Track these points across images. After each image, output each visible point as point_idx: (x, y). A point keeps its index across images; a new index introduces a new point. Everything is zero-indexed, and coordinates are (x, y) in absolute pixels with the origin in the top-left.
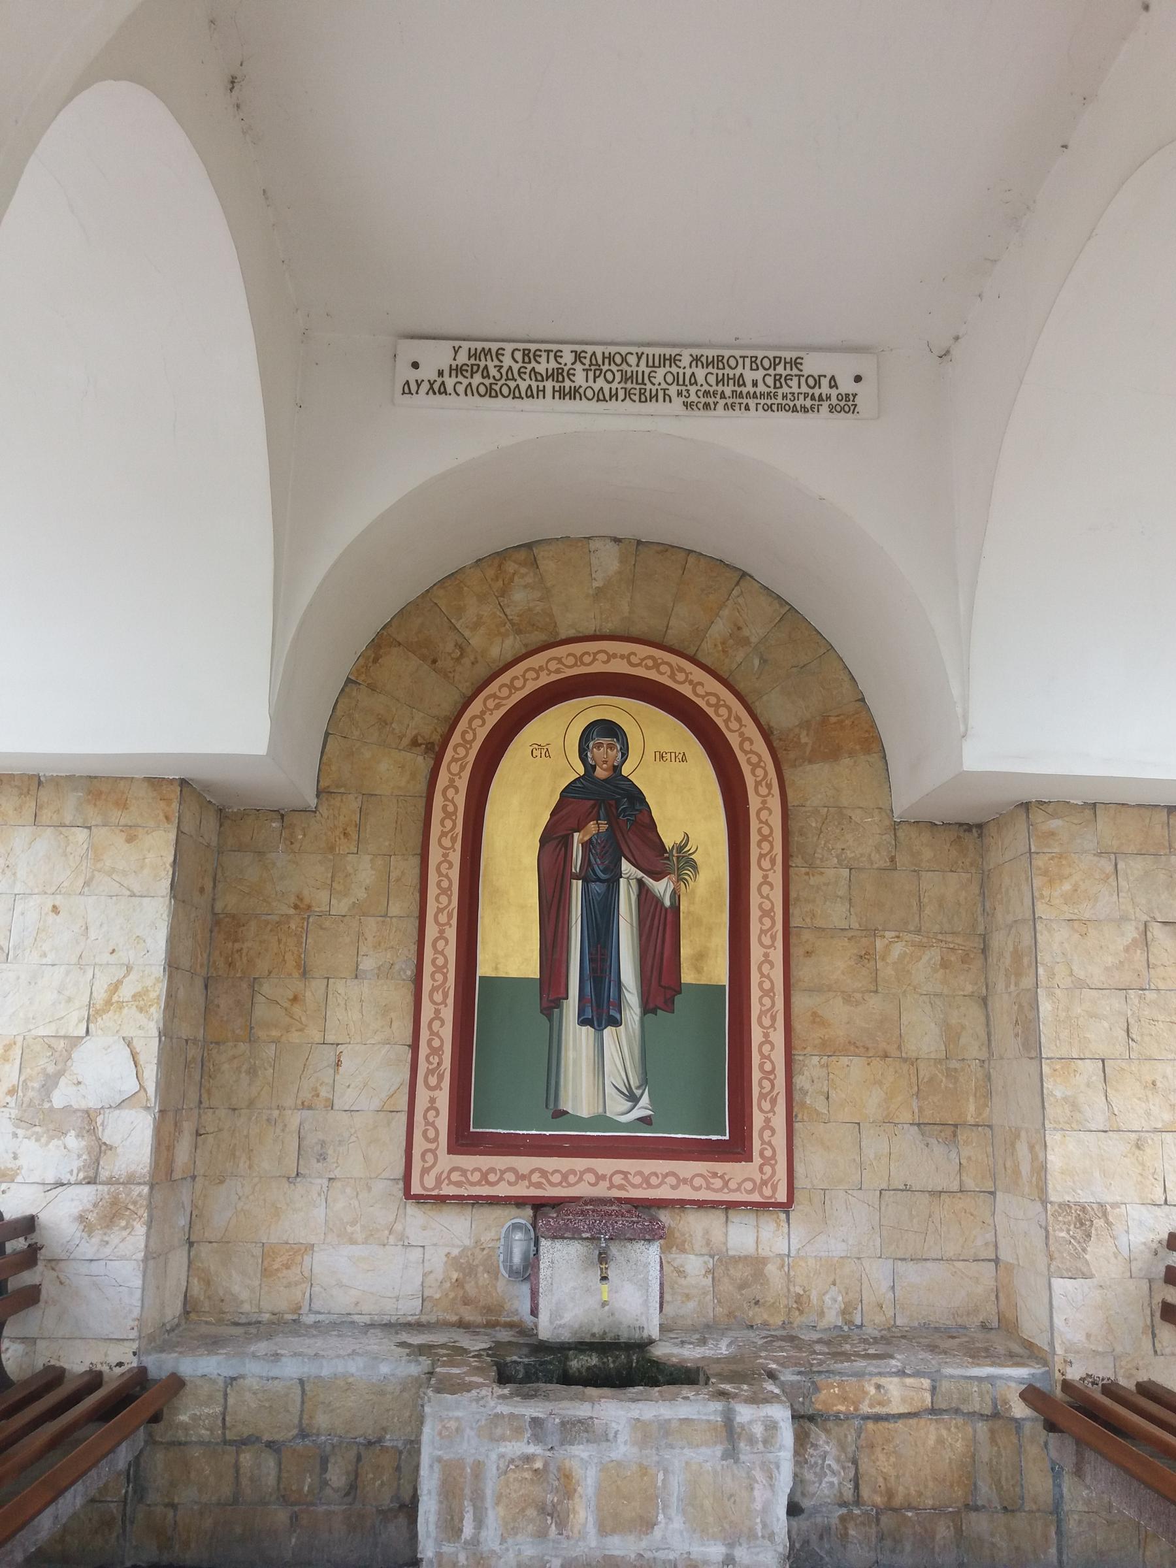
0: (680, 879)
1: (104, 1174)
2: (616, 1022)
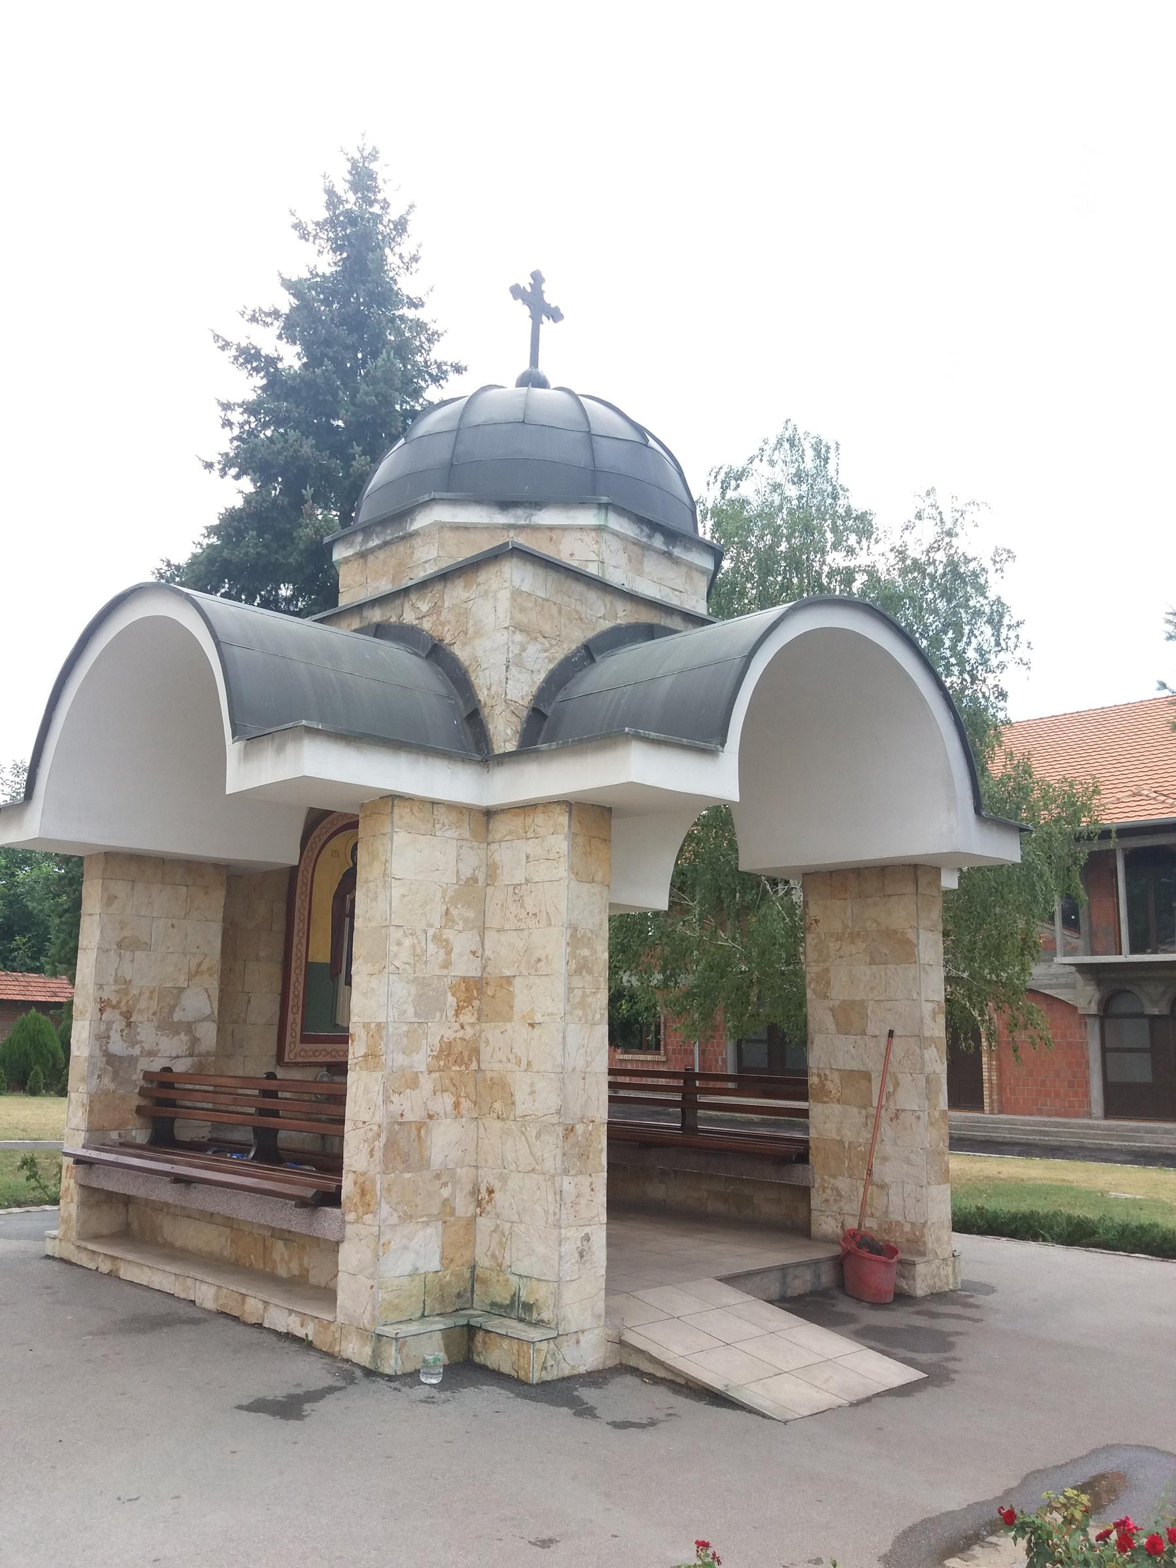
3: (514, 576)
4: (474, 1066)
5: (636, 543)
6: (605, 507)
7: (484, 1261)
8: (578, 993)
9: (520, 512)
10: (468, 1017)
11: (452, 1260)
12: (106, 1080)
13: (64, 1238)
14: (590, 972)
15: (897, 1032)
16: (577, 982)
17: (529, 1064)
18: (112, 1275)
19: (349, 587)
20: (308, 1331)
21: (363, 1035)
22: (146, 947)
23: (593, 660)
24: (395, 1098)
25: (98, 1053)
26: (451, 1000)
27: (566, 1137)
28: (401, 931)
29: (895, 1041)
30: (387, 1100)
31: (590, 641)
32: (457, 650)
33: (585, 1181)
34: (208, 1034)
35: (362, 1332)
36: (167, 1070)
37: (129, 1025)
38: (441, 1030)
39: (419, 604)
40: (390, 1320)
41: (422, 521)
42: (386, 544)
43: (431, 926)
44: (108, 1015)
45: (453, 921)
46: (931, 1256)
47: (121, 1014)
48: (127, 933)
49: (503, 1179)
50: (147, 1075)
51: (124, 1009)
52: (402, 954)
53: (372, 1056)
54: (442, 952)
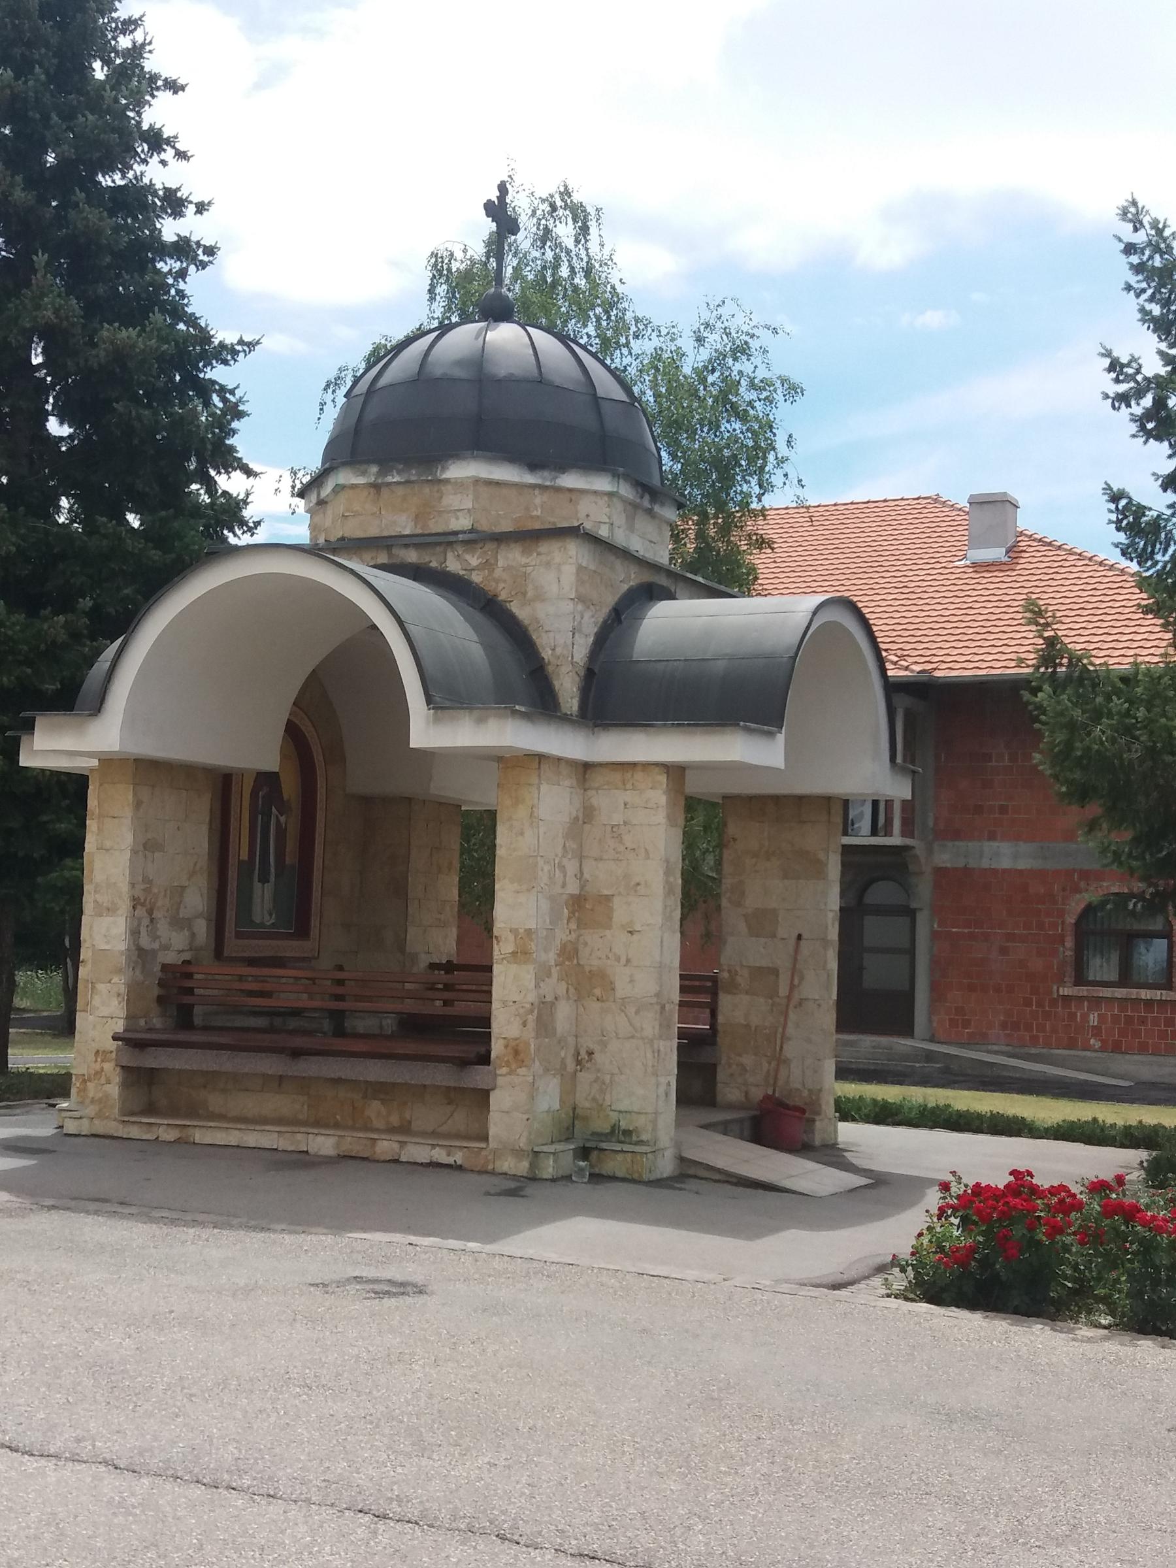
12: (138, 972)
13: (100, 1115)
17: (628, 961)
21: (511, 937)
37: (152, 920)
39: (468, 557)
50: (165, 967)
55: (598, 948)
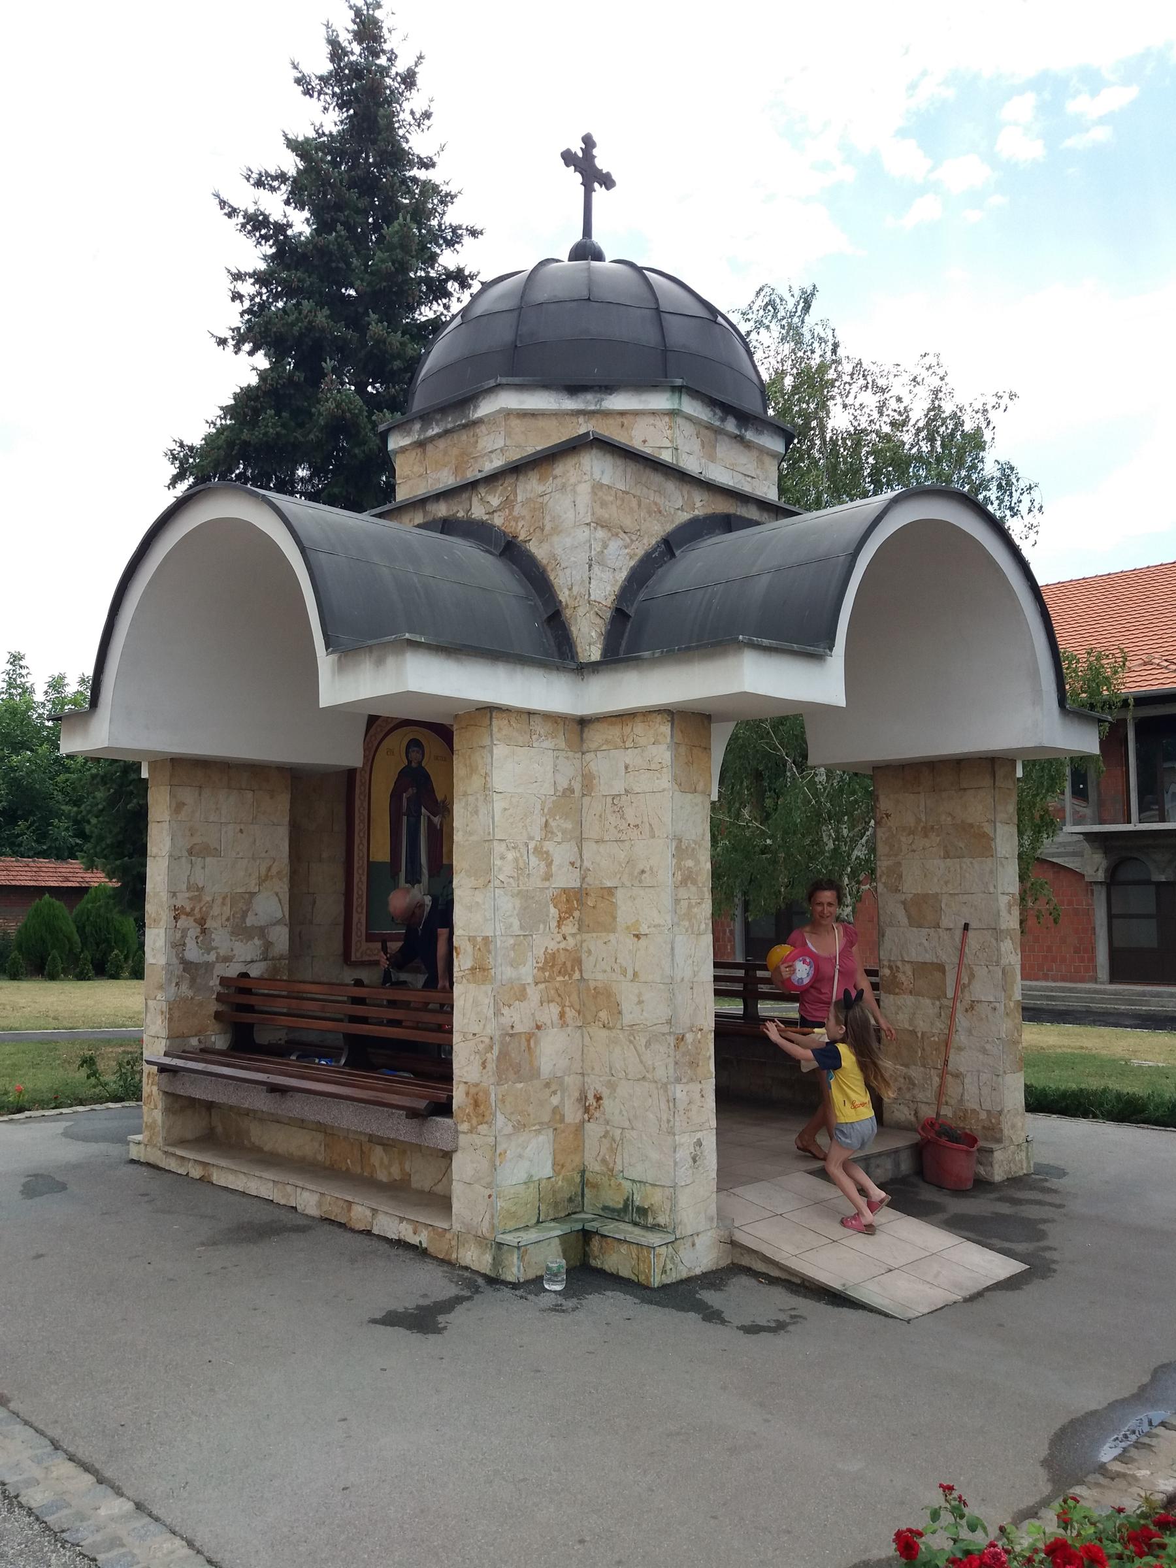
0: (444, 817)
1: (270, 956)
2: (419, 882)
3: (595, 468)
4: (577, 976)
5: (709, 427)
6: (677, 390)
7: (594, 1166)
8: (684, 904)
9: (589, 397)
10: (569, 928)
11: (563, 1166)
13: (149, 1143)
14: (694, 883)
15: (973, 925)
16: (683, 893)
17: (635, 974)
18: (204, 1180)
19: (408, 478)
20: (422, 1238)
21: (469, 948)
22: (216, 853)
23: (673, 555)
24: (505, 1011)
25: (175, 961)
26: (553, 911)
27: (677, 1047)
28: (504, 845)
29: (971, 934)
30: (498, 1013)
31: (670, 535)
32: (534, 548)
33: (695, 1087)
34: (281, 938)
35: (480, 1240)
36: (244, 975)
37: (203, 931)
38: (546, 941)
39: (489, 498)
40: (508, 1228)
41: (486, 408)
42: (447, 432)
43: (532, 838)
44: (183, 922)
45: (552, 833)
46: (1007, 1143)
47: (195, 920)
48: (197, 839)
49: (612, 1086)
50: (224, 981)
51: (198, 916)
52: (504, 868)
53: (480, 971)
54: (543, 864)
55: (603, 956)
